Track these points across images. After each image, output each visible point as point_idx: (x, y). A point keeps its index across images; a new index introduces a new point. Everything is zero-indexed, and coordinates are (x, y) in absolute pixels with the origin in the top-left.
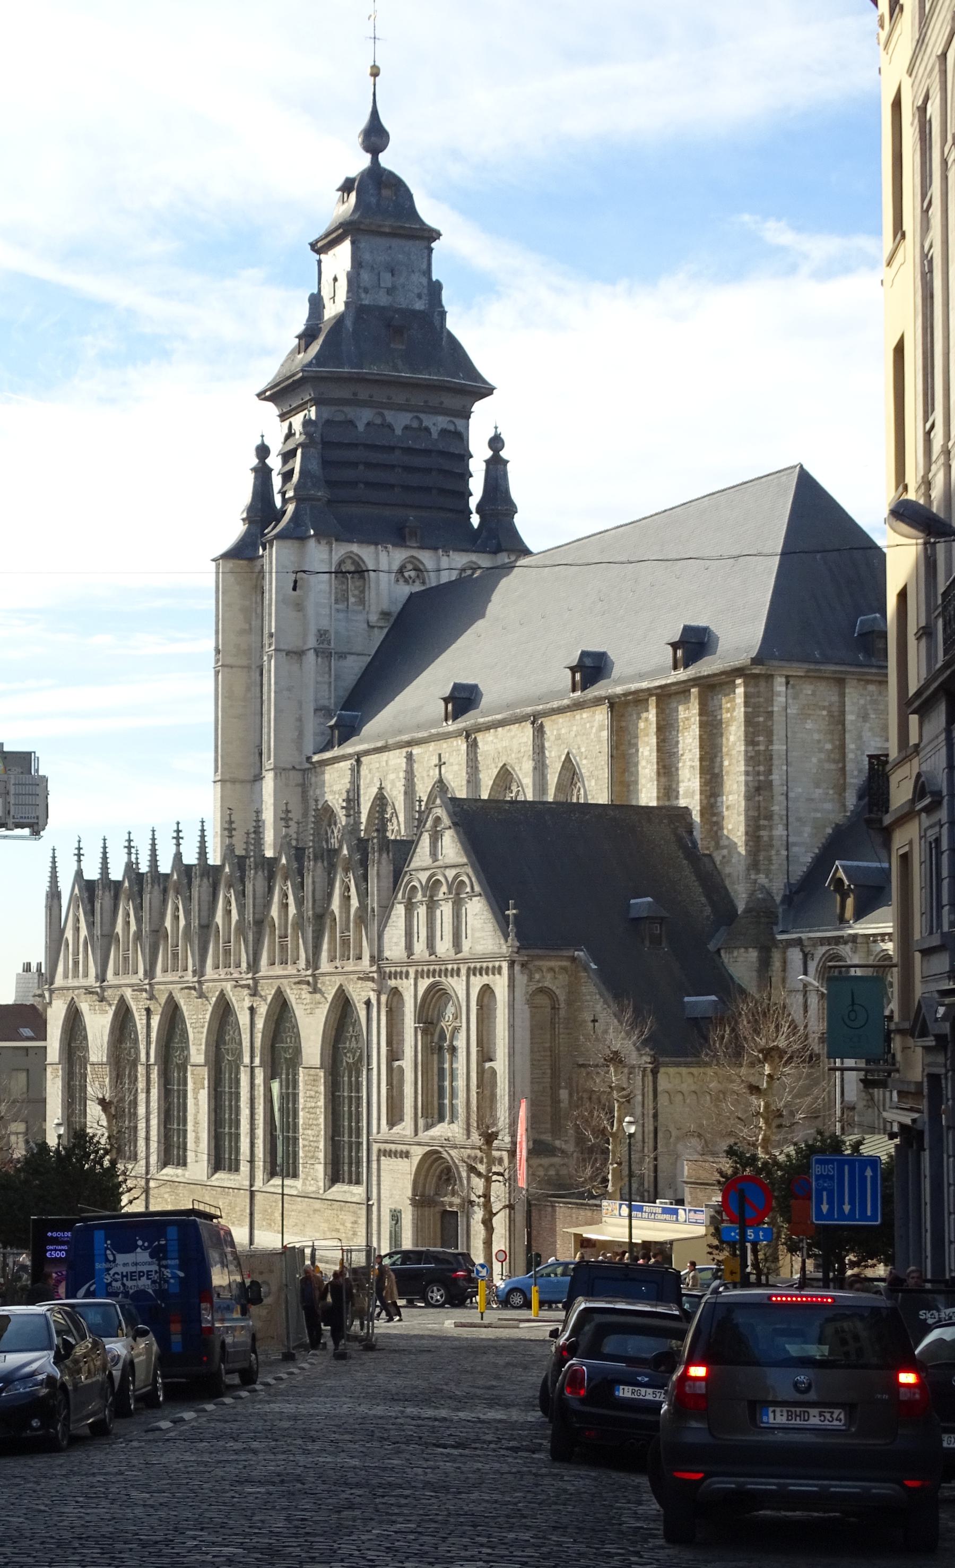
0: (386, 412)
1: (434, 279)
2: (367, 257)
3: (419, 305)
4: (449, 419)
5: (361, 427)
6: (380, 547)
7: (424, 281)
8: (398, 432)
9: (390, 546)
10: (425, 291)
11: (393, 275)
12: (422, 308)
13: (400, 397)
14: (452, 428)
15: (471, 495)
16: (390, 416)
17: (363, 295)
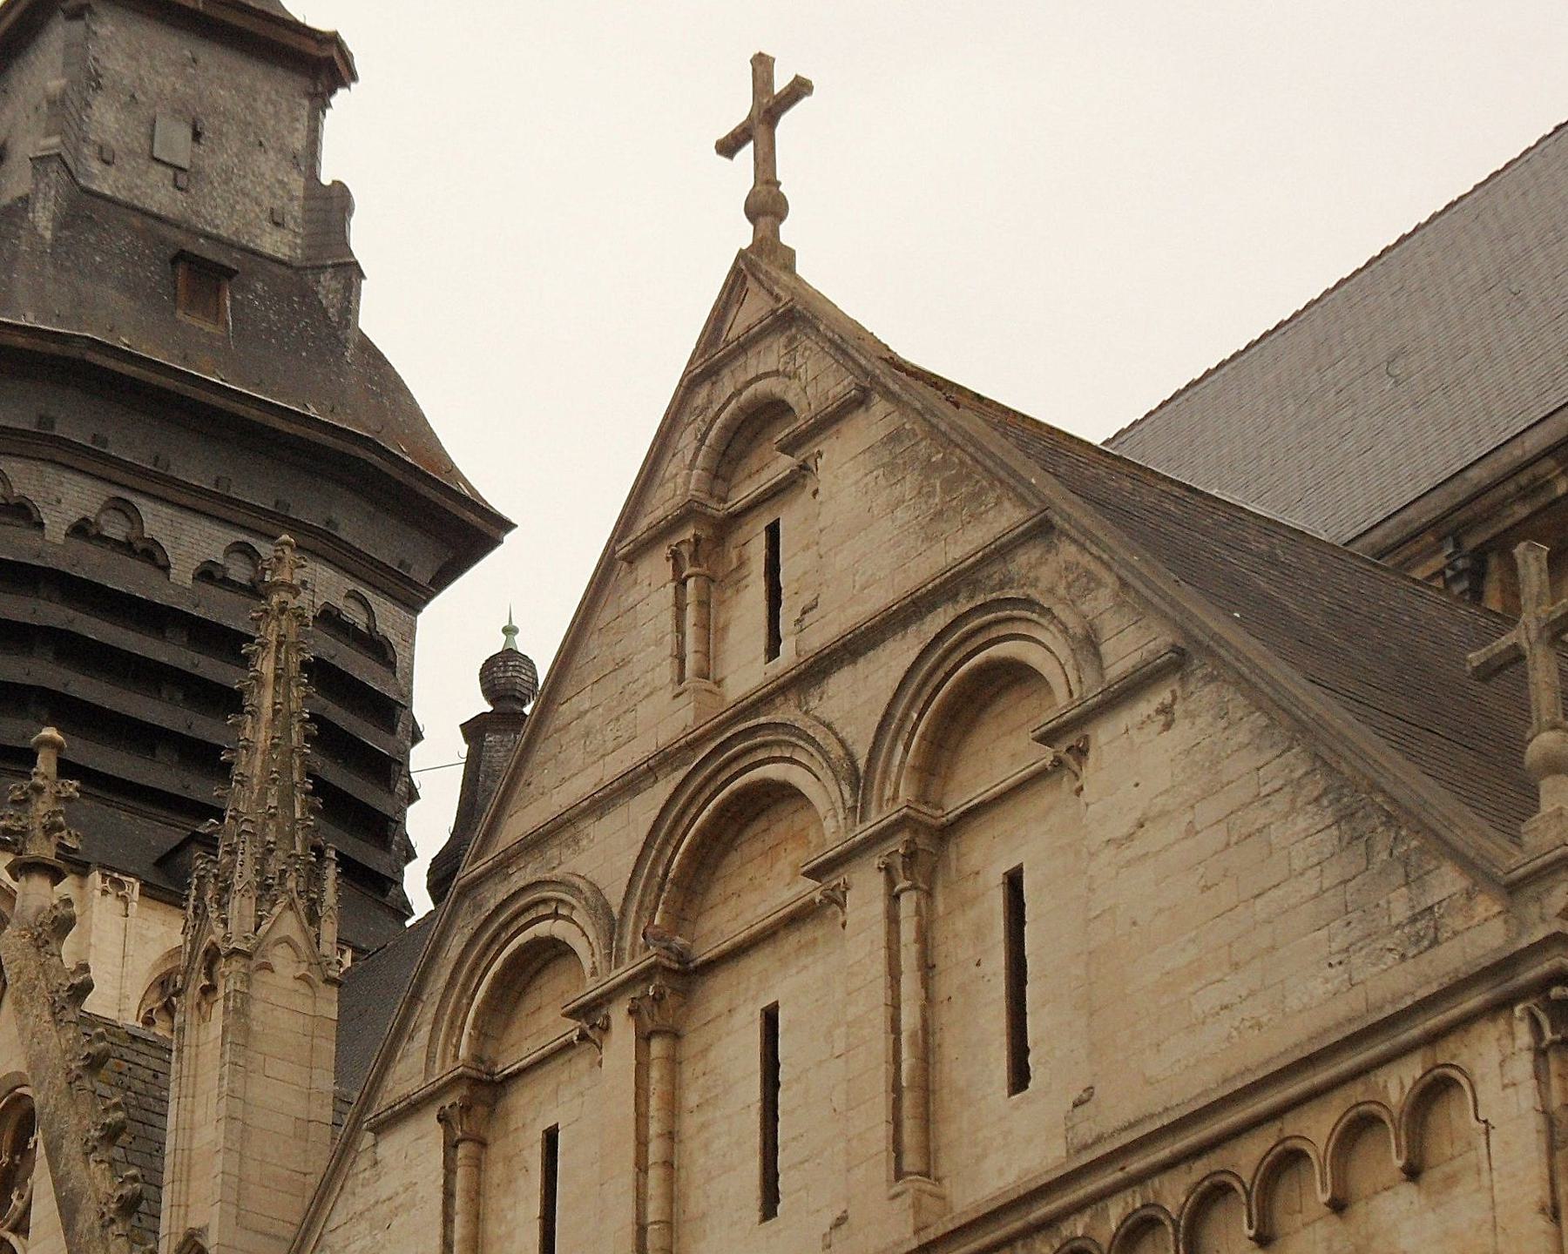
0: (145, 506)
1: (326, 179)
2: (116, 64)
3: (273, 243)
4: (352, 586)
5: (56, 525)
6: (96, 877)
7: (297, 184)
8: (183, 572)
9: (134, 888)
10: (296, 209)
11: (197, 136)
12: (283, 252)
13: (196, 469)
14: (361, 621)
15: (410, 855)
16: (156, 521)
17: (96, 167)
